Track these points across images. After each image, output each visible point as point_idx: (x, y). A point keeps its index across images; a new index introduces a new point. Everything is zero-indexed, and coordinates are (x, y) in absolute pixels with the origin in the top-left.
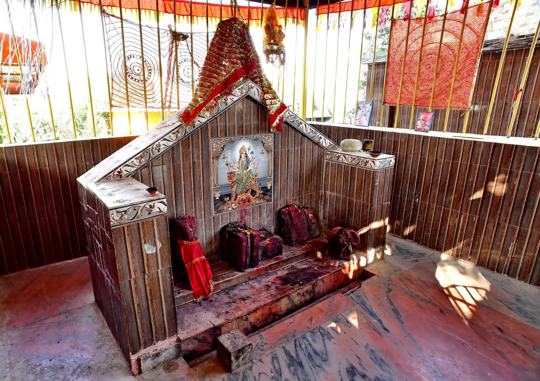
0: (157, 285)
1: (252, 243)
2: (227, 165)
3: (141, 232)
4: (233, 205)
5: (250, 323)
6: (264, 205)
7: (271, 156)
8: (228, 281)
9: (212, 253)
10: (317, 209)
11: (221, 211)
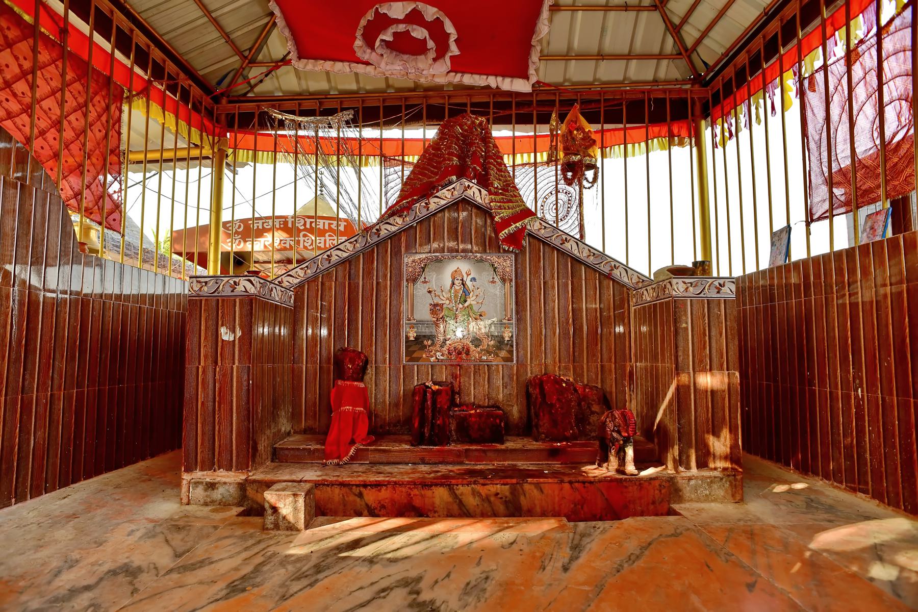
0: (229, 385)
1: (434, 403)
2: (430, 292)
3: (220, 311)
4: (438, 354)
5: (367, 505)
6: (497, 365)
7: (510, 288)
8: (384, 451)
9: (399, 421)
11: (418, 359)
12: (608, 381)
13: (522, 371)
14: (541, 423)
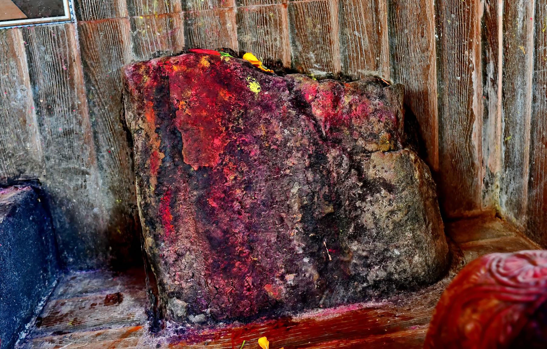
10: (452, 103)
12: (415, 56)
13: (98, 40)
14: (167, 251)
